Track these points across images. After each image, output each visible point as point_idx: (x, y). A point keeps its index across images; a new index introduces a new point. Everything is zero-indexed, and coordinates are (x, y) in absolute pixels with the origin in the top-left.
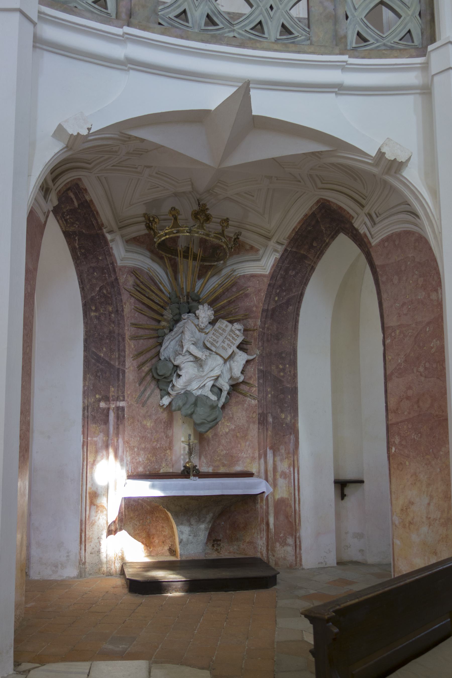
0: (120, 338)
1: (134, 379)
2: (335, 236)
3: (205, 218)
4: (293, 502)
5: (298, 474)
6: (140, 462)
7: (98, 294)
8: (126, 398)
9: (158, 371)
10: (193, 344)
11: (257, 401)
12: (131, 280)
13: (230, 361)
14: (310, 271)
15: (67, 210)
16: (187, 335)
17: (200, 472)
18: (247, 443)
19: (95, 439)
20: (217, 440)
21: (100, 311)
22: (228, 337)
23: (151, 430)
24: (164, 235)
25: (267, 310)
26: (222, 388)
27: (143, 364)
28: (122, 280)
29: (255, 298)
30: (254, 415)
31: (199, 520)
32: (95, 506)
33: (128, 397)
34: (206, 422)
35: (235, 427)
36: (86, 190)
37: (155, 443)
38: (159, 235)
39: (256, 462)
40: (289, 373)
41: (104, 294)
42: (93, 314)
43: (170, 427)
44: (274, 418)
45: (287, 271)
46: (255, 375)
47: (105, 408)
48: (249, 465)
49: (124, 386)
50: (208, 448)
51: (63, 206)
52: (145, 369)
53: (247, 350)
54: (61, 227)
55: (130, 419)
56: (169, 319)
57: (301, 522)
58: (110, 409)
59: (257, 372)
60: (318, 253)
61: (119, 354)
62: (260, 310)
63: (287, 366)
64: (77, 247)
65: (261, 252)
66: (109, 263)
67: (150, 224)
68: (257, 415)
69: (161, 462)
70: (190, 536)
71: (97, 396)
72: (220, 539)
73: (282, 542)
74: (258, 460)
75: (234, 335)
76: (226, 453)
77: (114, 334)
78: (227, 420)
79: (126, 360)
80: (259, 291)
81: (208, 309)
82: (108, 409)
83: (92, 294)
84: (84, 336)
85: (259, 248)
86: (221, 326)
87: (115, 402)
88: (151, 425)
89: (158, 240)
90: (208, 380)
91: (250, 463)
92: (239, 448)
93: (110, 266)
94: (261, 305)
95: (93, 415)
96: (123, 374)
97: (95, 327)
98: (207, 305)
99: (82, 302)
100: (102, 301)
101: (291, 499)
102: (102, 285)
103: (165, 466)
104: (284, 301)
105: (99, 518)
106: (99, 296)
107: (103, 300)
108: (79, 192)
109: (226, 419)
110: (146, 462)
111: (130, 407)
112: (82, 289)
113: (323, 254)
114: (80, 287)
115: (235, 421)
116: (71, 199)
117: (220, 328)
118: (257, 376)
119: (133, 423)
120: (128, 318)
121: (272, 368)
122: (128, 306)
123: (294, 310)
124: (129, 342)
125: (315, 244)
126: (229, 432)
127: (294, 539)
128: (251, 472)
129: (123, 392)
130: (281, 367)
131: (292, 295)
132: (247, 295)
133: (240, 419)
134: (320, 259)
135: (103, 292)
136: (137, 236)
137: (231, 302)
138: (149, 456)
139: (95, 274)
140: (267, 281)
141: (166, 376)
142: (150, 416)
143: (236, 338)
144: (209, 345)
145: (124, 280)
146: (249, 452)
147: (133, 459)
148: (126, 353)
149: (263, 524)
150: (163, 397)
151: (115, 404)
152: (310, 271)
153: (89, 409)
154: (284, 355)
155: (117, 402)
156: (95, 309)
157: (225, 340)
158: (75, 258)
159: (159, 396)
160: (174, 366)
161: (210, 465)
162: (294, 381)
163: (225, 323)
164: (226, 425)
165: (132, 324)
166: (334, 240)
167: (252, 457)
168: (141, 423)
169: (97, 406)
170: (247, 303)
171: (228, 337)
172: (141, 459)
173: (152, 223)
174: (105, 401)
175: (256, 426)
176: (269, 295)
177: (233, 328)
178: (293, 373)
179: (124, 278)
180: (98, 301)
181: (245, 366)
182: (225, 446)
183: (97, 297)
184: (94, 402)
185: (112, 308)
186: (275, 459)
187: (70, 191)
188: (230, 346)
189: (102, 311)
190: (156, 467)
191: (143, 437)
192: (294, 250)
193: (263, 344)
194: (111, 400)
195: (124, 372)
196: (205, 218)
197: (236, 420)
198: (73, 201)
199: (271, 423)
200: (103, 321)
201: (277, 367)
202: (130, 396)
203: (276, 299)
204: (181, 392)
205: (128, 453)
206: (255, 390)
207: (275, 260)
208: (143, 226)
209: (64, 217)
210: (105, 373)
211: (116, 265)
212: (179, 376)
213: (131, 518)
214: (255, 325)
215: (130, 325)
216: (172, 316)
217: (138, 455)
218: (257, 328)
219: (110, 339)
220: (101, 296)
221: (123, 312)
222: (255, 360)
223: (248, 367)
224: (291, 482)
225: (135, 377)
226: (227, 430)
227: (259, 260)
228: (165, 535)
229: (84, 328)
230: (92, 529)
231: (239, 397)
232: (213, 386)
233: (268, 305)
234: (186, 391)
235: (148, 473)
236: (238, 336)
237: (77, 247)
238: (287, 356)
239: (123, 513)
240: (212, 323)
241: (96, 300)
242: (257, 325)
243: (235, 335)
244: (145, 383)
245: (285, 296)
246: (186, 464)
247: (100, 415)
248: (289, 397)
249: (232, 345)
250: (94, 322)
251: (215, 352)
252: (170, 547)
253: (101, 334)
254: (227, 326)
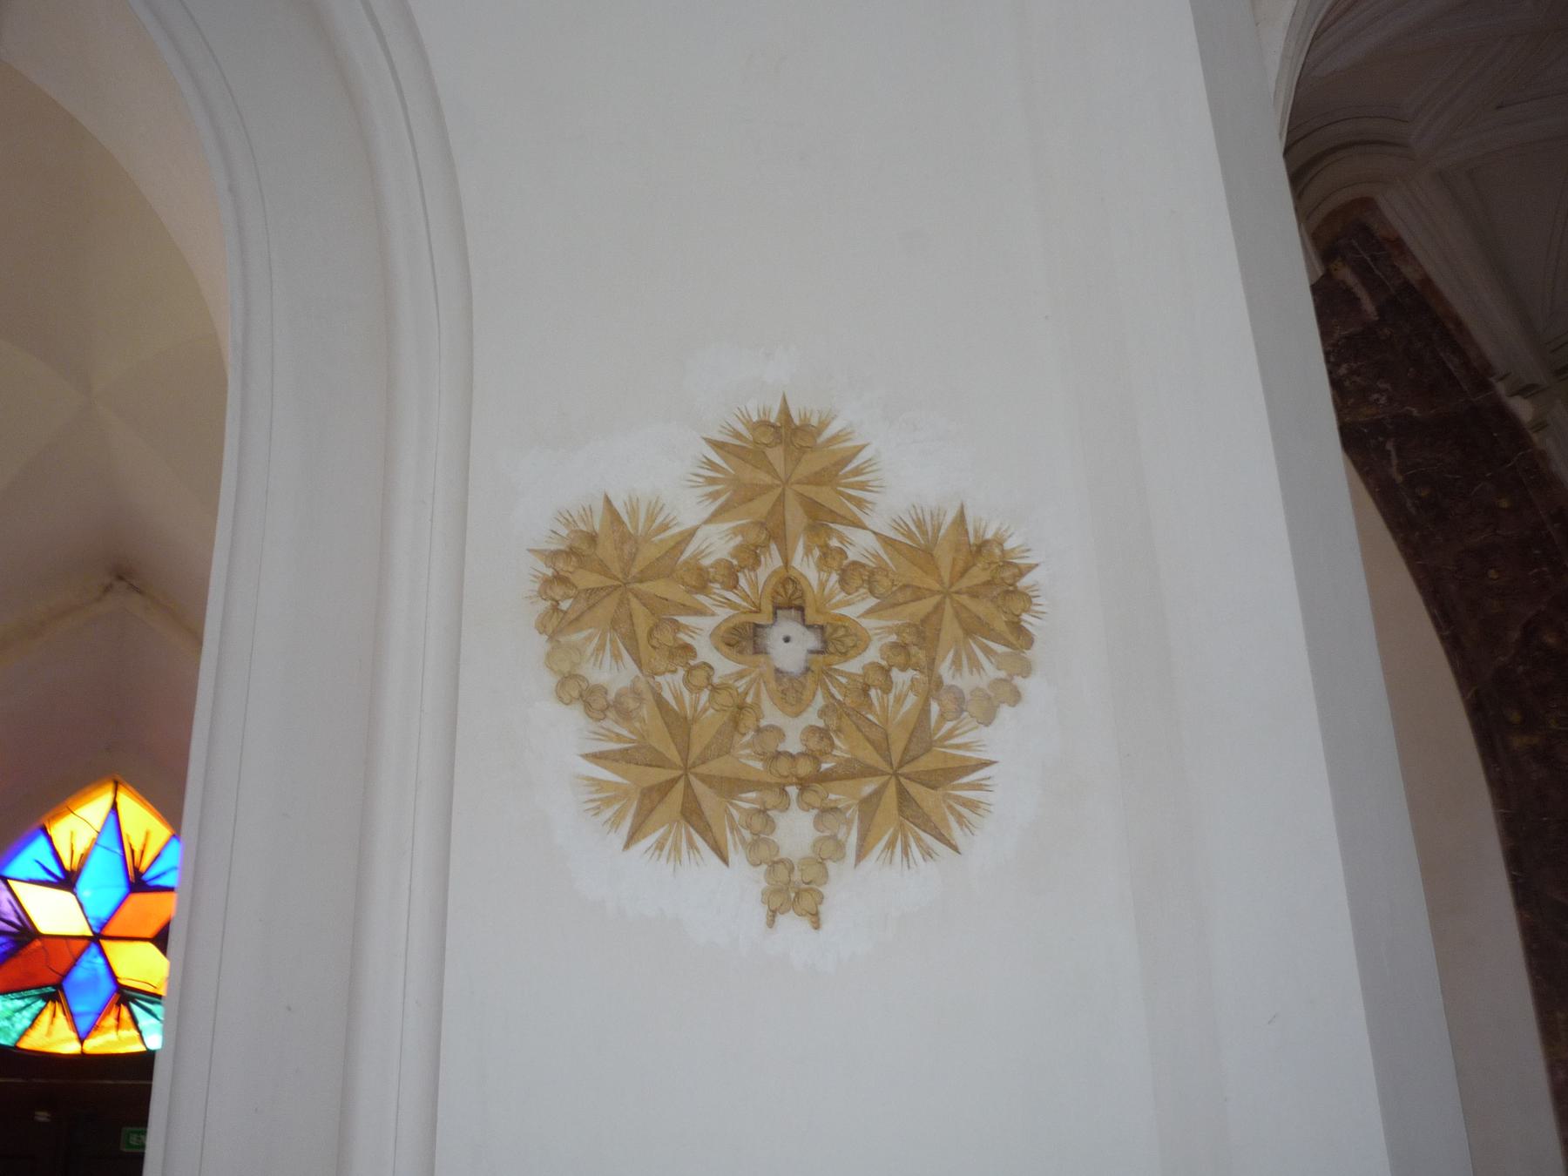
36: (1398, 243)
64: (1399, 479)
116: (1348, 291)
139: (1492, 574)
183: (1521, 669)
237: (1399, 479)
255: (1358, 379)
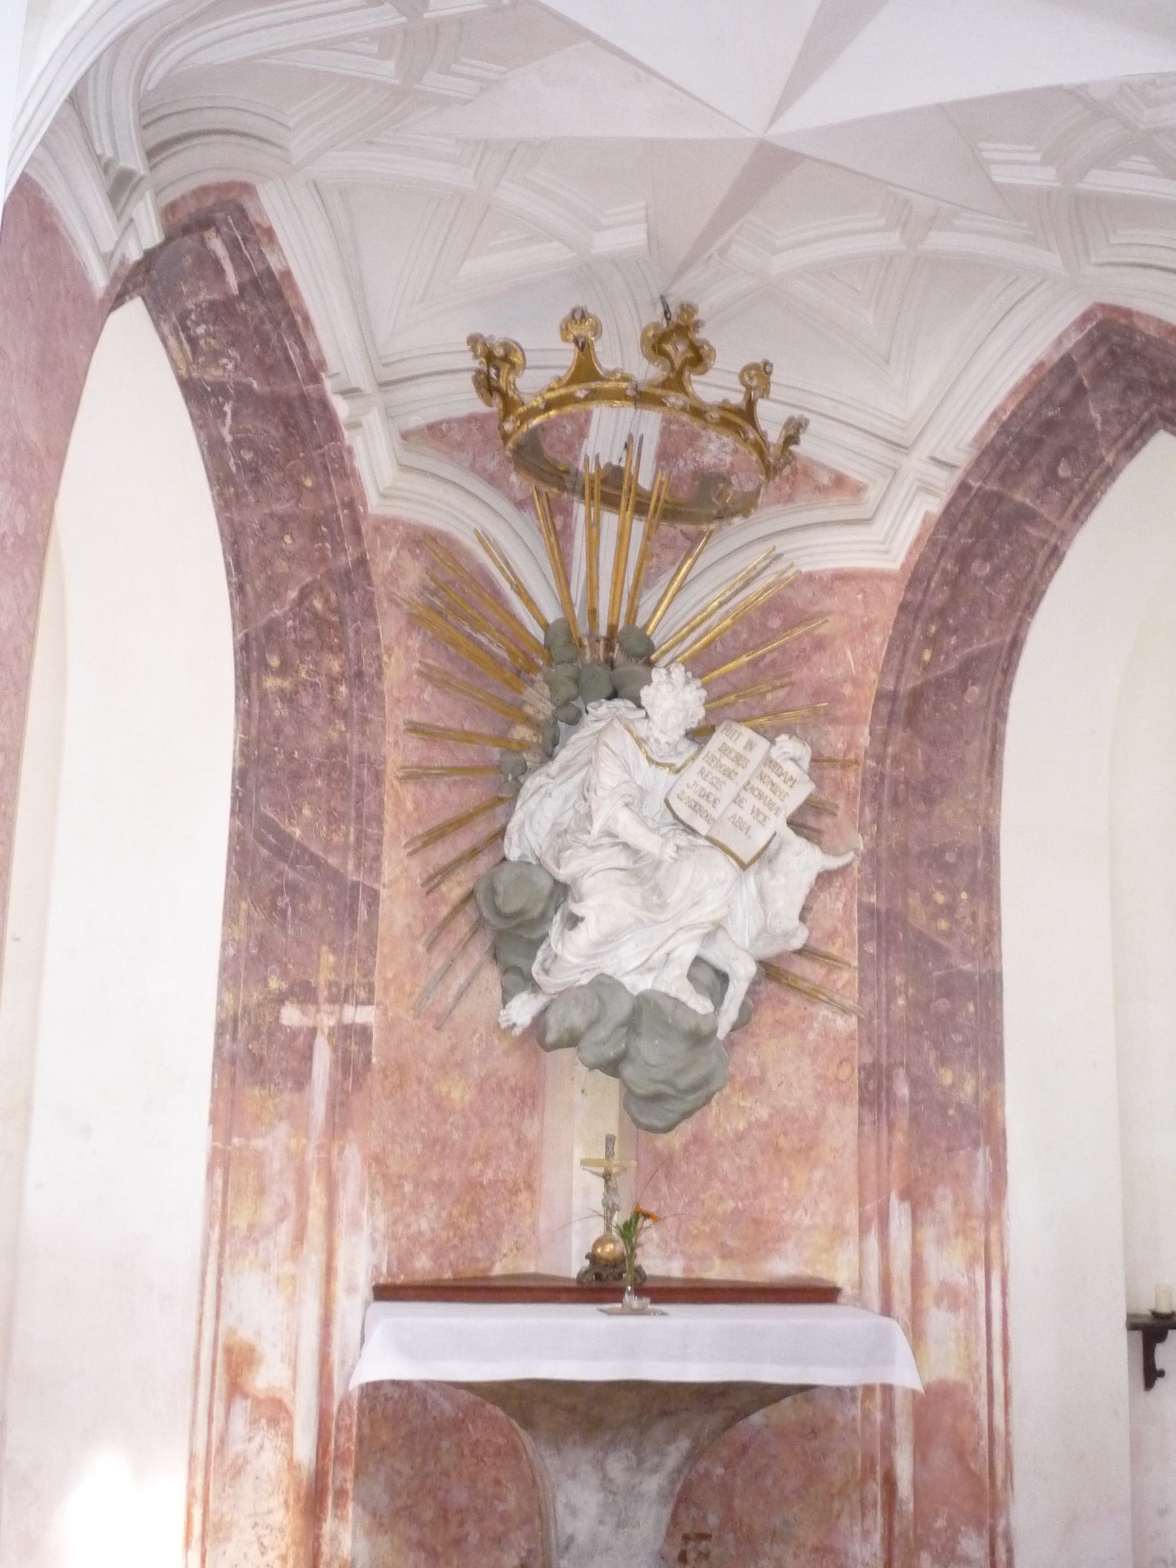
0: (365, 771)
1: (409, 926)
2: (1137, 443)
3: (690, 355)
4: (983, 1401)
5: (1004, 1294)
6: (421, 1233)
7: (293, 614)
8: (378, 995)
9: (499, 901)
10: (627, 805)
11: (854, 1019)
12: (413, 574)
13: (758, 872)
14: (1046, 564)
15: (197, 306)
16: (609, 776)
17: (644, 1278)
18: (818, 1175)
19: (258, 1143)
20: (703, 1159)
21: (297, 672)
22: (756, 783)
23: (464, 1117)
24: (542, 406)
25: (893, 697)
26: (727, 969)
27: (446, 872)
28: (381, 567)
29: (849, 654)
30: (845, 1072)
31: (640, 1462)
32: (249, 1402)
33: (386, 990)
34: (670, 1091)
35: (771, 1116)
36: (269, 233)
37: (479, 1165)
38: (521, 410)
39: (851, 1246)
40: (969, 921)
41: (315, 614)
42: (271, 683)
43: (534, 1106)
44: (915, 1084)
45: (964, 559)
46: (848, 925)
47: (300, 1029)
48: (824, 1256)
49: (372, 949)
50: (669, 1186)
51: (184, 289)
52: (450, 890)
53: (820, 832)
54: (173, 361)
55: (389, 1073)
56: (541, 717)
57: (1015, 1477)
58: (319, 1033)
59: (856, 915)
60: (1076, 502)
61: (360, 833)
62: (870, 694)
63: (964, 896)
65: (872, 495)
66: (338, 502)
67: (493, 372)
68: (856, 1071)
69: (499, 1236)
70: (601, 1522)
71: (274, 984)
72: (707, 1531)
73: (939, 1548)
74: (857, 1238)
75: (779, 776)
76: (736, 1208)
77: (344, 757)
78: (742, 1089)
79: (385, 854)
80: (867, 627)
81: (687, 682)
82: (313, 1032)
83: (271, 610)
84: (234, 760)
85: (865, 481)
86: (730, 744)
87: (337, 1007)
88: (467, 1097)
89: (519, 427)
90: (681, 937)
91: (827, 1250)
92: (785, 1193)
93: (343, 514)
94: (873, 676)
95: (255, 1051)
96: (369, 905)
97: (278, 730)
98: (683, 669)
99: (234, 635)
100: (306, 637)
101: (976, 1388)
102: (309, 579)
103: (511, 1250)
104: (952, 666)
105: (261, 1447)
106: (294, 620)
107: (309, 634)
108: (245, 240)
109: (737, 1086)
110: (444, 1235)
111: (390, 1026)
112: (238, 590)
113: (1094, 506)
114: (230, 584)
115: (770, 1091)
116: (217, 261)
117: (724, 750)
118: (855, 928)
119: (401, 1086)
120: (399, 701)
121: (911, 901)
122: (398, 660)
123: (989, 699)
124: (399, 788)
125: (1063, 471)
126: (748, 1130)
127: (985, 1541)
128: (827, 1281)
129: (368, 973)
130: (940, 898)
131: (978, 646)
132: (820, 644)
133: (791, 1084)
134: (1082, 523)
135: (313, 607)
136: (441, 423)
137: (761, 665)
138: (455, 1212)
139: (288, 539)
140: (893, 594)
141: (527, 917)
142: (461, 1065)
143: (784, 787)
144: (684, 812)
145: (388, 567)
146: (822, 1207)
147: (395, 1222)
148: (387, 828)
149: (875, 1480)
150: (512, 996)
151: (337, 1015)
152: (1046, 564)
153: (240, 1031)
154: (950, 858)
155: (346, 1006)
156: (281, 666)
157: (743, 794)
158: (219, 478)
159: (497, 993)
160: (556, 882)
161: (674, 1252)
162: (990, 952)
163: (746, 733)
164: (739, 1106)
165: (414, 728)
166: (1132, 457)
167: (835, 1228)
168: (429, 1089)
169: (269, 1019)
170: (822, 670)
171: (756, 783)
172: (424, 1225)
173: (498, 369)
174: (300, 1002)
175: (852, 1111)
176: (900, 641)
177: (775, 753)
178: (986, 920)
179: (390, 558)
180: (293, 636)
181: (812, 895)
182: (733, 1184)
183: (290, 623)
184: (260, 1005)
185: (341, 662)
186: (919, 1236)
187: (213, 229)
188: (761, 817)
189: (303, 675)
190: (480, 1254)
191: (435, 1141)
192: (992, 486)
193: (879, 814)
194: (321, 999)
195: (374, 898)
196: (690, 355)
197: (774, 1088)
198: (220, 271)
199: (907, 1101)
200: (305, 711)
201: (927, 899)
202: (392, 989)
203: (927, 656)
204: (579, 980)
205: (378, 1201)
206: (848, 981)
207: (924, 521)
208: (466, 383)
209: (185, 329)
210: (307, 899)
211: (362, 509)
212: (574, 921)
213: (383, 1449)
214: (850, 746)
215: (402, 727)
216: (554, 708)
217: (416, 1206)
218: (857, 755)
219: (329, 774)
220: (303, 621)
221: (380, 679)
222: (849, 870)
223: (823, 896)
224: (977, 1323)
225: (415, 916)
226: (742, 1125)
227: (867, 521)
228: (504, 1511)
229: (236, 731)
230: (231, 1491)
231: (786, 1003)
232: (698, 961)
233: (898, 679)
234: (598, 976)
235: (448, 1275)
236: (792, 781)
238: (961, 862)
239: (354, 1430)
240: (699, 735)
241: (286, 634)
242: (857, 748)
243: (782, 778)
244: (449, 942)
245: (955, 648)
246: (595, 1246)
247: (282, 1054)
248: (971, 1008)
249: (771, 815)
250: (272, 711)
251: (708, 838)
252: (521, 1559)
253: (296, 755)
254: (750, 746)
255: (212, 342)
